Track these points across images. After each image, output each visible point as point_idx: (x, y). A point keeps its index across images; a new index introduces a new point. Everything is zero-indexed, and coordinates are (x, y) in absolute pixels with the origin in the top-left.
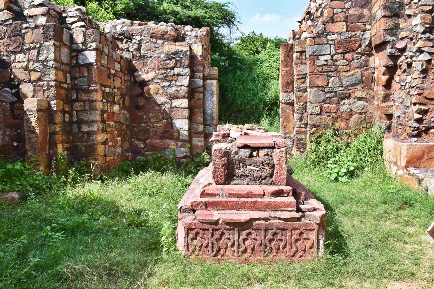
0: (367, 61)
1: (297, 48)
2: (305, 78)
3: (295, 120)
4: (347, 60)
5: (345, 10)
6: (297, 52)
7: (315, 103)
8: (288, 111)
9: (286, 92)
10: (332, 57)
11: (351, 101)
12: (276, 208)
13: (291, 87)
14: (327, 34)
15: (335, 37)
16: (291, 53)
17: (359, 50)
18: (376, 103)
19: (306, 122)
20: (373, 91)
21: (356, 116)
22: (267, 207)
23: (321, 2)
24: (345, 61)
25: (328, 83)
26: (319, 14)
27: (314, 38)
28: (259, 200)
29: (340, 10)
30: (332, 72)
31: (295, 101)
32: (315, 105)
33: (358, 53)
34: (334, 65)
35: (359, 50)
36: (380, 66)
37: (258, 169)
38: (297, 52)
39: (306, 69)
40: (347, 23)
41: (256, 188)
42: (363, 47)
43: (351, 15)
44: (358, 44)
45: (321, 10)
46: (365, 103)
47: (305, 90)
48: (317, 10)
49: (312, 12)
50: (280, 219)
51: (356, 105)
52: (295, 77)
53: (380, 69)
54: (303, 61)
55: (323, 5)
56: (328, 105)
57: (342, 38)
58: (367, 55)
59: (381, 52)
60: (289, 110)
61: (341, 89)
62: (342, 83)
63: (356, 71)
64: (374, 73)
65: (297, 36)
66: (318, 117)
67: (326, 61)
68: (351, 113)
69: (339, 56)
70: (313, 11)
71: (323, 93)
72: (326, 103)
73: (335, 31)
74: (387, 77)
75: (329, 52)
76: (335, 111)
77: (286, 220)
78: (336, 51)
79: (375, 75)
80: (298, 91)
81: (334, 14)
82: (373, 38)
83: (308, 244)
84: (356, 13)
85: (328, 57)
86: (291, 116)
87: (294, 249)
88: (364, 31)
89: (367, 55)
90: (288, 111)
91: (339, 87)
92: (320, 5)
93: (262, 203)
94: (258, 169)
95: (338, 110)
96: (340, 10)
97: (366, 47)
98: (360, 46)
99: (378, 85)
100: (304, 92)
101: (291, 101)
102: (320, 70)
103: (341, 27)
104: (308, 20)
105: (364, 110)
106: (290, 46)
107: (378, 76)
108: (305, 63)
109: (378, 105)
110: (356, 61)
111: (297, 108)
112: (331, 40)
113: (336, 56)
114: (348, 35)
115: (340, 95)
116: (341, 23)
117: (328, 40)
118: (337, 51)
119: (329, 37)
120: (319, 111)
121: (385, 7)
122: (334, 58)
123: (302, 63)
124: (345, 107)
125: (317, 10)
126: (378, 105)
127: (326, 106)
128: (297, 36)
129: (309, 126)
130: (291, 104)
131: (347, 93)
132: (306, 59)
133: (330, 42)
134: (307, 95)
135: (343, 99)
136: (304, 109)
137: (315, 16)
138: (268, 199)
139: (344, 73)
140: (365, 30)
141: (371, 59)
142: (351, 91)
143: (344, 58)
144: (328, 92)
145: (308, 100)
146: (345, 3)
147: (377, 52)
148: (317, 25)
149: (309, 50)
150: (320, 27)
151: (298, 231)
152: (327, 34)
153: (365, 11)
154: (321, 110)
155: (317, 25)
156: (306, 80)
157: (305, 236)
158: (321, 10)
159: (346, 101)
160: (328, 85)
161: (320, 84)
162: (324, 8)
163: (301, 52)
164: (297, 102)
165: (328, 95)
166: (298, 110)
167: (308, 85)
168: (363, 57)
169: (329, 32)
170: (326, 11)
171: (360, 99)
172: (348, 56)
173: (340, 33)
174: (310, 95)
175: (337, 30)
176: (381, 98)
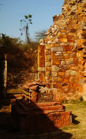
0: (75, 55)
1: (47, 48)
2: (50, 61)
3: (46, 79)
4: (68, 54)
5: (67, 33)
6: (46, 49)
7: (55, 72)
8: (42, 75)
9: (41, 67)
10: (62, 52)
11: (70, 71)
12: (57, 109)
13: (44, 64)
14: (60, 43)
15: (63, 44)
16: (43, 49)
17: (72, 50)
18: (80, 72)
19: (51, 80)
20: (78, 66)
21: (72, 77)
22: (53, 109)
23: (56, 28)
24: (67, 54)
25: (61, 63)
26: (56, 34)
27: (54, 44)
28: (51, 107)
29: (65, 33)
30: (62, 58)
31: (46, 71)
32: (55, 73)
33: (72, 51)
34: (63, 56)
35: (72, 50)
36: (81, 56)
37: (48, 97)
38: (46, 49)
39: (49, 57)
40: (67, 39)
41: (49, 103)
42: (74, 49)
43: (69, 36)
44: (72, 48)
45: (56, 32)
46: (75, 72)
47: (50, 66)
48: (55, 32)
49: (52, 32)
50: (58, 112)
51: (72, 73)
52: (46, 60)
53: (81, 58)
54: (49, 54)
55: (58, 30)
56: (61, 73)
57: (66, 45)
58: (76, 52)
59: (81, 50)
60: (43, 75)
61: (65, 66)
62: (66, 63)
63: (71, 58)
64: (78, 59)
65: (46, 42)
66: (57, 78)
67: (59, 54)
68: (70, 76)
69: (65, 52)
70: (53, 32)
71: (58, 67)
72: (59, 72)
73: (63, 41)
74: (84, 61)
75: (60, 50)
76: (63, 75)
77: (60, 112)
78: (63, 50)
79: (79, 60)
80: (47, 66)
81: (62, 35)
82: (78, 45)
83: (67, 119)
84: (71, 35)
85: (60, 52)
86: (44, 78)
87: (63, 122)
88: (74, 42)
89: (76, 52)
90: (42, 75)
91: (65, 65)
92: (56, 30)
93: (51, 108)
94: (48, 97)
95: (65, 74)
96: (65, 33)
97: (75, 49)
98: (73, 48)
99: (80, 64)
100: (50, 67)
101: (43, 71)
102: (57, 58)
103: (66, 40)
104: (51, 35)
105: (75, 75)
106: (43, 46)
107: (80, 61)
108: (50, 54)
109: (81, 72)
110: (71, 54)
111: (47, 74)
112: (62, 45)
113: (64, 52)
114: (68, 44)
115: (65, 68)
116: (65, 39)
117: (60, 45)
118: (64, 50)
119: (60, 44)
120: (57, 75)
121: (82, 35)
122: (63, 53)
123: (49, 54)
124: (67, 73)
125: (55, 32)
126: (81, 72)
127: (60, 73)
128: (46, 42)
129: (52, 82)
130: (44, 72)
131: (68, 68)
132: (50, 53)
133: (61, 46)
134: (51, 68)
135: (66, 70)
136: (50, 74)
137: (54, 34)
138: (53, 106)
139: (67, 59)
140: (75, 42)
141: (77, 53)
142: (69, 67)
143: (67, 53)
144: (60, 67)
145: (52, 70)
146: (67, 30)
147: (79, 50)
148: (55, 38)
149: (52, 50)
150: (57, 40)
151: (64, 115)
152: (60, 43)
153: (75, 35)
154: (58, 75)
155: (55, 38)
156: (51, 62)
157: (66, 117)
158: (56, 32)
159: (68, 71)
160: (60, 64)
161: (57, 64)
162: (58, 31)
163: (48, 50)
164: (47, 71)
165: (61, 68)
166: (47, 75)
167: (52, 64)
168: (74, 53)
169: (60, 42)
170: (59, 33)
171: (73, 70)
172: (68, 52)
173: (65, 43)
174: (53, 68)
175: (64, 42)
176: (82, 69)
